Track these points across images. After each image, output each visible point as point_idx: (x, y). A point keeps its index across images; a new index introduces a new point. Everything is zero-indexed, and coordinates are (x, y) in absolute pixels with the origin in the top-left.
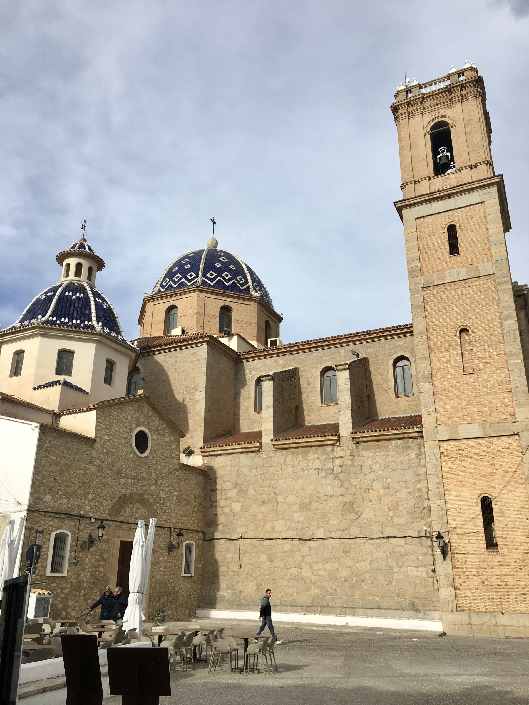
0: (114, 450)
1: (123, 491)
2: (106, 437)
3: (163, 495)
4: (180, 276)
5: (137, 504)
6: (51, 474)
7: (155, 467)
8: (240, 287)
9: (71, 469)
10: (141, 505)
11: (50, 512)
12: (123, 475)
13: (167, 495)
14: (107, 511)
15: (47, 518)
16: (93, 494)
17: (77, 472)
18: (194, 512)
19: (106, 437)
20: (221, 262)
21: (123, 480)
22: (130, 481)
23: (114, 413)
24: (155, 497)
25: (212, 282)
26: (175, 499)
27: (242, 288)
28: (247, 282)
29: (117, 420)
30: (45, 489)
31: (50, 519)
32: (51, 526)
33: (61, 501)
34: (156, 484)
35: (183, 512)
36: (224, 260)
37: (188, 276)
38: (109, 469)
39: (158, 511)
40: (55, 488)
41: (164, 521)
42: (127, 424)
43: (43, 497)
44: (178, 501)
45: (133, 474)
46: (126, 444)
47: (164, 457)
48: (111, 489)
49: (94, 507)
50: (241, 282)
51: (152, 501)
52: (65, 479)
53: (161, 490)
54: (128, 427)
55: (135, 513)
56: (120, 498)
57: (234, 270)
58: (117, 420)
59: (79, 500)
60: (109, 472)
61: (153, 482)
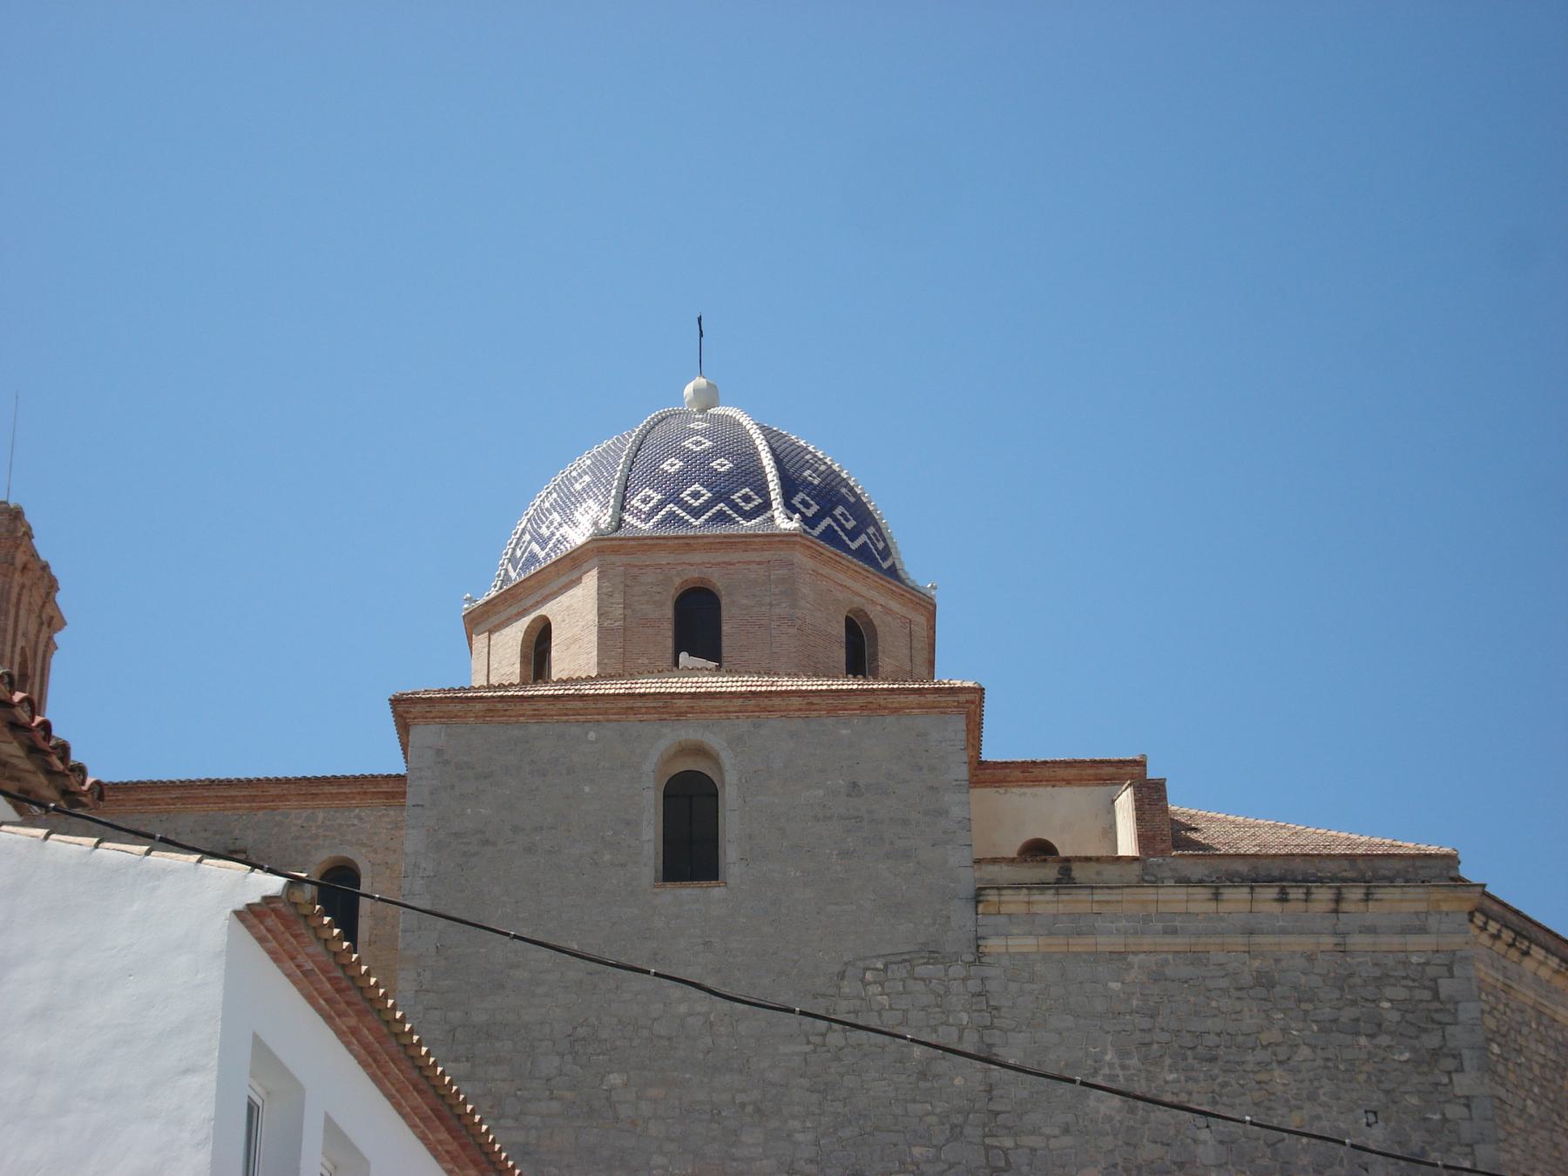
20: (686, 456)
36: (698, 443)
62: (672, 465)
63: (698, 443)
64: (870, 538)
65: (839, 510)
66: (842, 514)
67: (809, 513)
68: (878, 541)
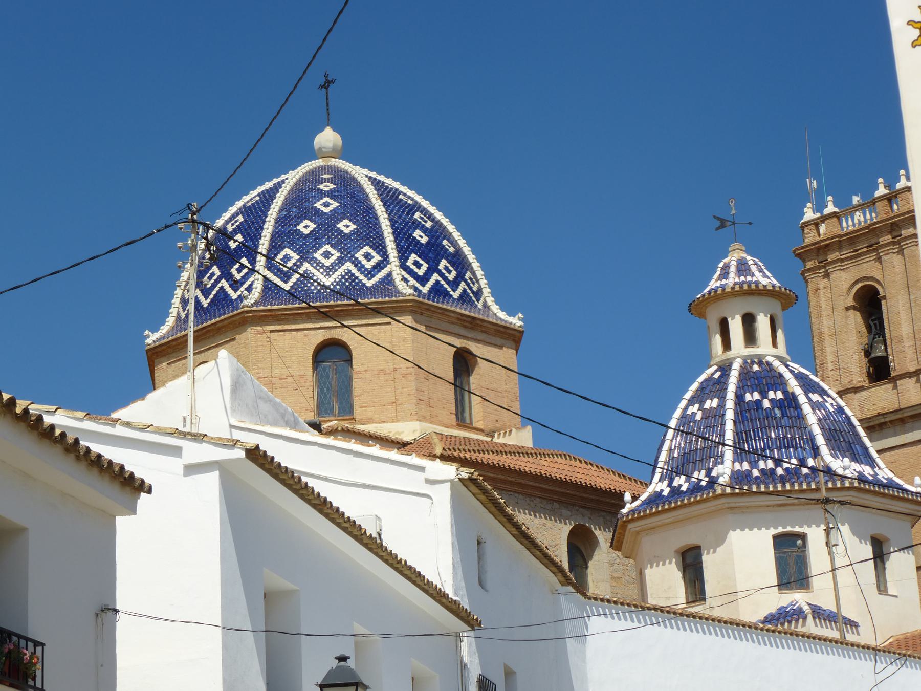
4: (218, 273)
8: (365, 281)
25: (286, 282)
27: (369, 284)
28: (385, 260)
36: (326, 205)
37: (233, 271)
50: (369, 265)
57: (353, 233)
62: (306, 227)
63: (326, 205)
64: (468, 285)
65: (443, 263)
66: (446, 268)
67: (421, 272)
68: (474, 283)
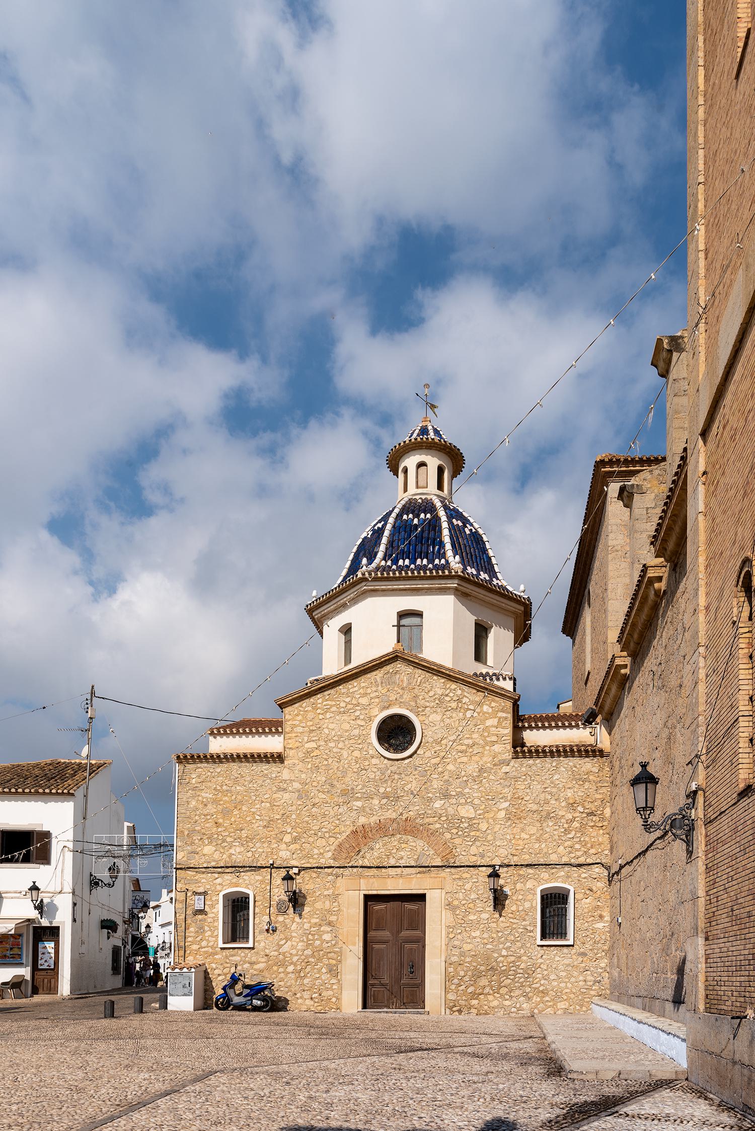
0: (330, 760)
1: (362, 820)
2: (313, 745)
3: (466, 812)
5: (399, 836)
6: (209, 817)
7: (440, 769)
9: (243, 805)
10: (409, 837)
11: (214, 868)
12: (359, 795)
13: (479, 812)
14: (330, 854)
15: (209, 875)
16: (294, 833)
17: (258, 806)
18: (567, 831)
19: (313, 745)
21: (359, 804)
22: (376, 802)
23: (324, 703)
24: (444, 819)
26: (502, 814)
29: (332, 712)
30: (201, 839)
31: (216, 875)
32: (219, 884)
33: (232, 851)
34: (446, 796)
35: (531, 835)
38: (323, 792)
39: (457, 841)
40: (218, 835)
41: (475, 855)
42: (357, 713)
43: (200, 849)
44: (513, 817)
45: (382, 790)
46: (360, 746)
47: (464, 747)
48: (331, 821)
49: (299, 852)
51: (438, 826)
52: (233, 819)
53: (461, 804)
54: (362, 717)
55: (395, 851)
56: (355, 832)
58: (332, 712)
59: (266, 845)
60: (324, 797)
61: (438, 795)
